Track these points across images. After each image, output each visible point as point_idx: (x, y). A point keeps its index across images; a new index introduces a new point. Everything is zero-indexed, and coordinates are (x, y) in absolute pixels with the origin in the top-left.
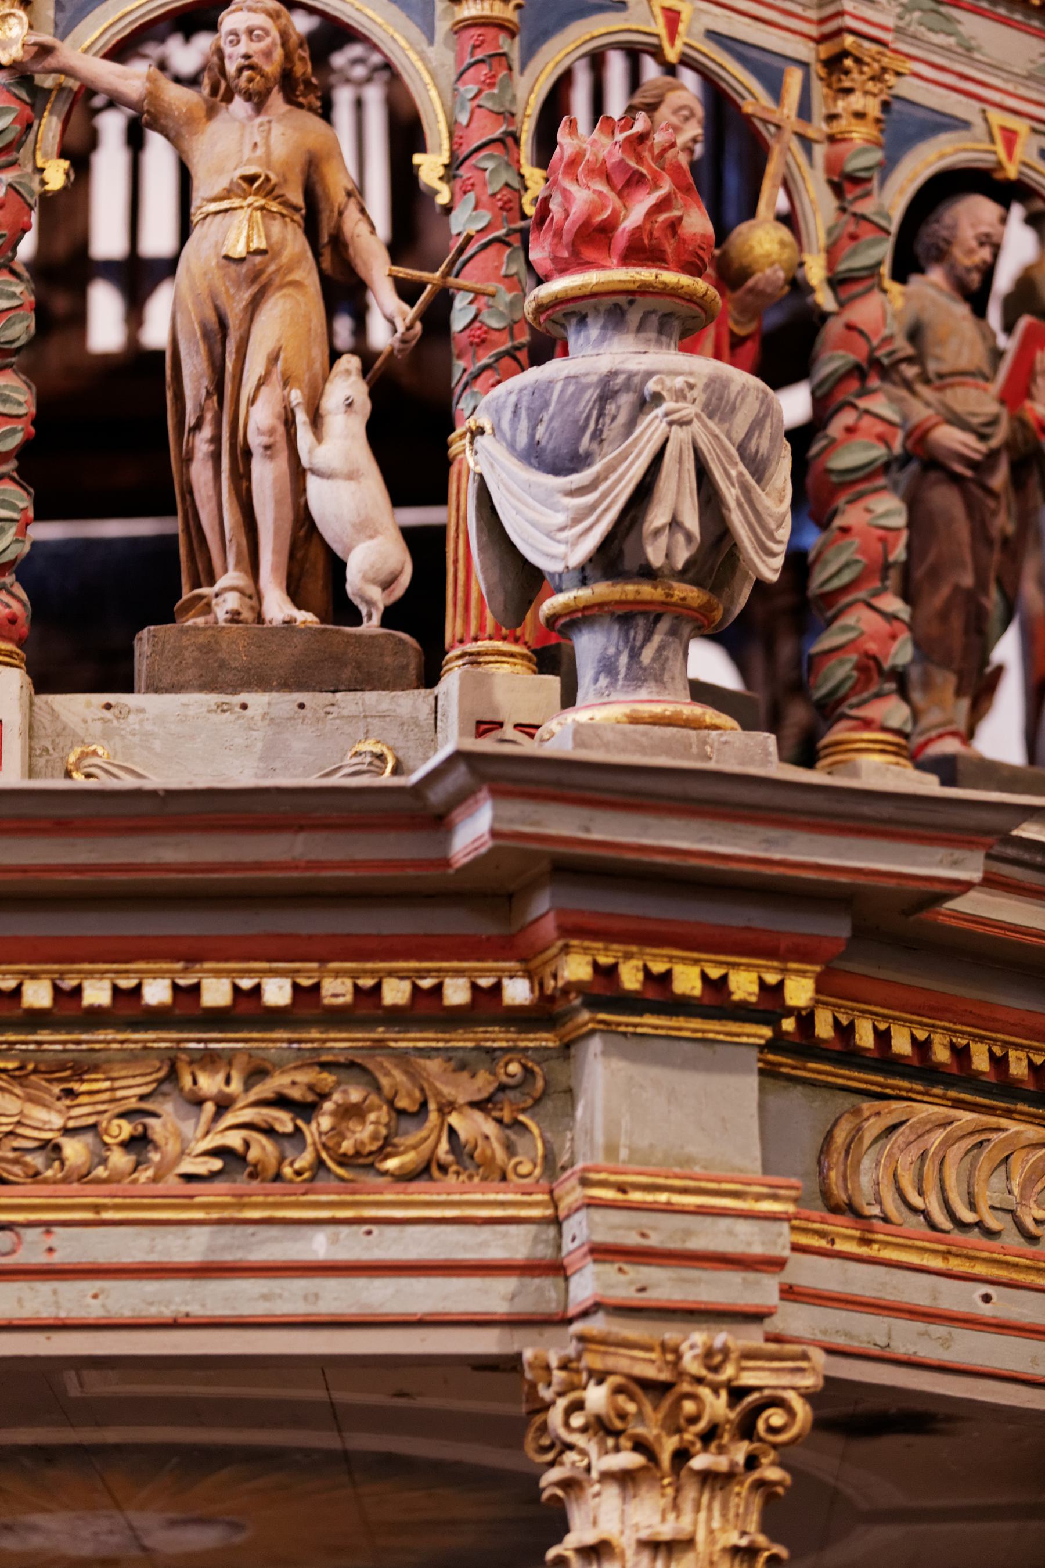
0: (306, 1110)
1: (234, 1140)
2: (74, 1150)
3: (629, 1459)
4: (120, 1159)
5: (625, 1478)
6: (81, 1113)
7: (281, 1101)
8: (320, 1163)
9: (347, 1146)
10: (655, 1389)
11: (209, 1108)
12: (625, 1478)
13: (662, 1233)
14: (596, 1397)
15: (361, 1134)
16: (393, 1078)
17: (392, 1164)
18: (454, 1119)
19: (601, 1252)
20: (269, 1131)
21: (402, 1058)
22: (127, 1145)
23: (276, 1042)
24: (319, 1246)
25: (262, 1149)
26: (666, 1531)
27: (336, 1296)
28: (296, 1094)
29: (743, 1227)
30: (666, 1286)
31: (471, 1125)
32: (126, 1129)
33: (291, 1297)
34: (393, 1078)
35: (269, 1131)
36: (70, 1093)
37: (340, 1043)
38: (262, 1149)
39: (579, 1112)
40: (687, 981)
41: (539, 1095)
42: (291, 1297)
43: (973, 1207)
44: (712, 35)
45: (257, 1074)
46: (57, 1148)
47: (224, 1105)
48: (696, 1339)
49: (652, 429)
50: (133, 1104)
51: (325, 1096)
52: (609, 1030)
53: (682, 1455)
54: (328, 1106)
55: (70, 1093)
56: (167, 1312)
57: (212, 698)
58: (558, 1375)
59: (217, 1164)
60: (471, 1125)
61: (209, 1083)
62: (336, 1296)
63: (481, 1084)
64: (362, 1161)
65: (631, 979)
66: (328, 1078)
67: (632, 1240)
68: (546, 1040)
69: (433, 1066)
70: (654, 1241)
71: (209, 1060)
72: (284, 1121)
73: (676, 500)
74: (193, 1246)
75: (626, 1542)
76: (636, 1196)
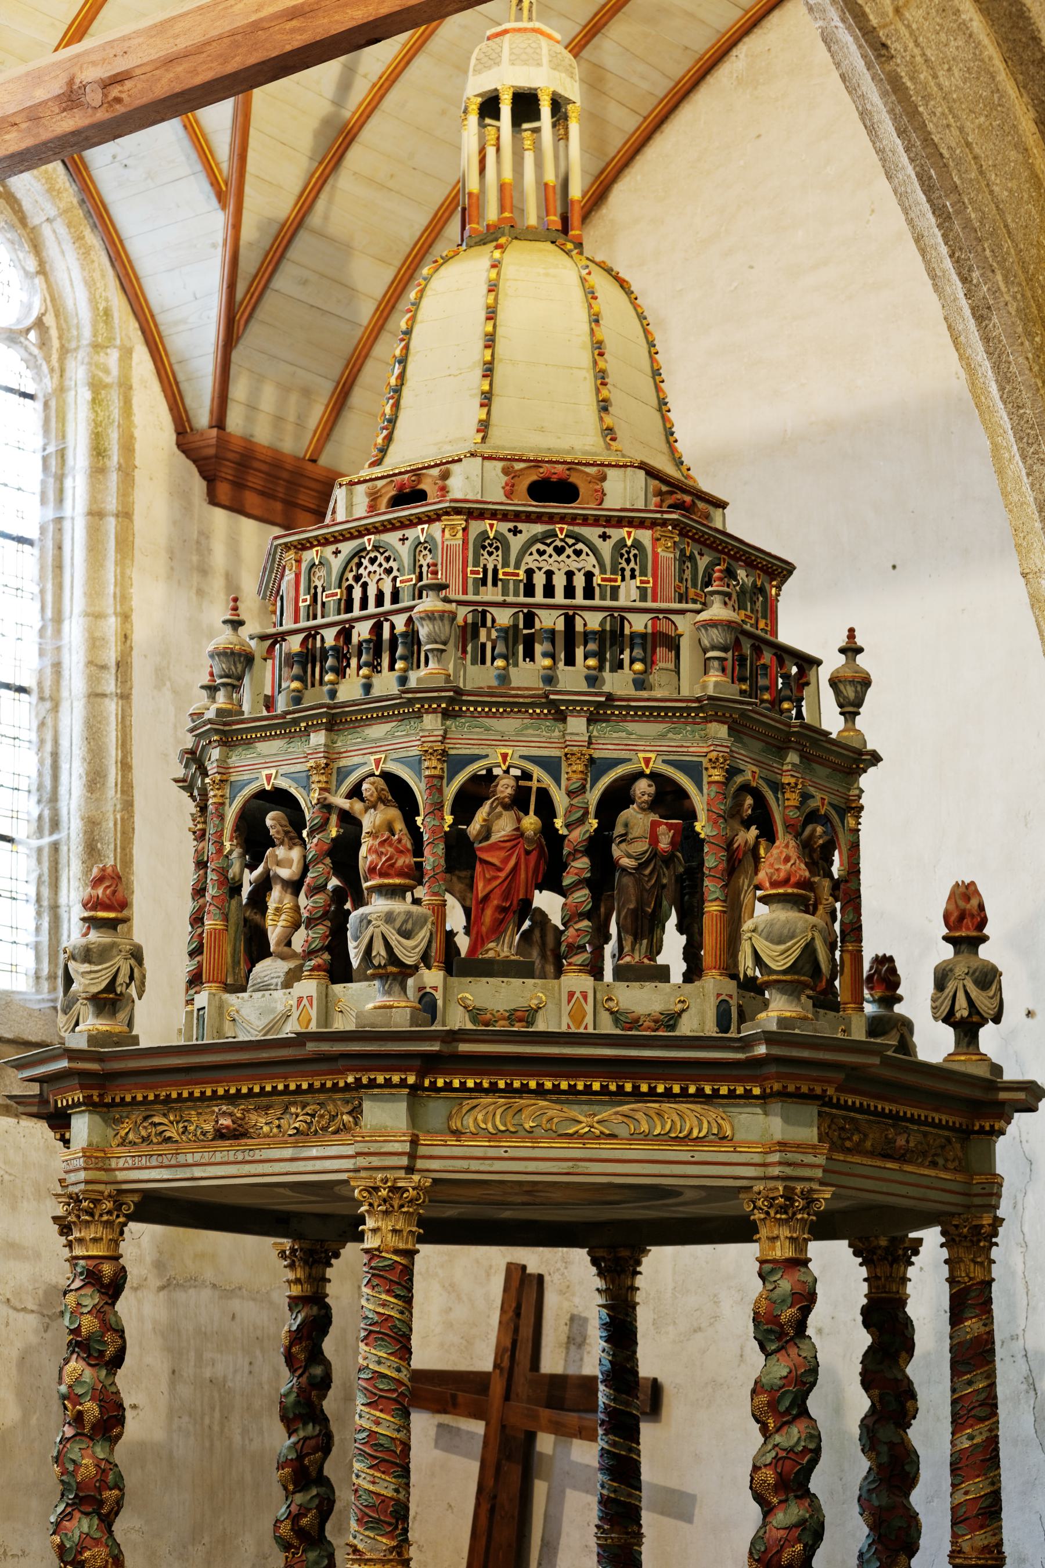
0: (313, 1116)
4: (275, 1130)
13: (374, 1148)
16: (331, 1107)
21: (334, 1101)
23: (308, 1098)
24: (314, 1152)
27: (319, 1165)
29: (396, 1145)
30: (376, 1161)
33: (310, 1166)
40: (380, 1080)
41: (356, 1112)
42: (310, 1166)
44: (521, 757)
47: (297, 1116)
49: (371, 928)
57: (367, 983)
61: (293, 1110)
62: (319, 1165)
63: (350, 1107)
64: (324, 1129)
65: (365, 1081)
71: (294, 1104)
73: (379, 948)
74: (288, 1153)
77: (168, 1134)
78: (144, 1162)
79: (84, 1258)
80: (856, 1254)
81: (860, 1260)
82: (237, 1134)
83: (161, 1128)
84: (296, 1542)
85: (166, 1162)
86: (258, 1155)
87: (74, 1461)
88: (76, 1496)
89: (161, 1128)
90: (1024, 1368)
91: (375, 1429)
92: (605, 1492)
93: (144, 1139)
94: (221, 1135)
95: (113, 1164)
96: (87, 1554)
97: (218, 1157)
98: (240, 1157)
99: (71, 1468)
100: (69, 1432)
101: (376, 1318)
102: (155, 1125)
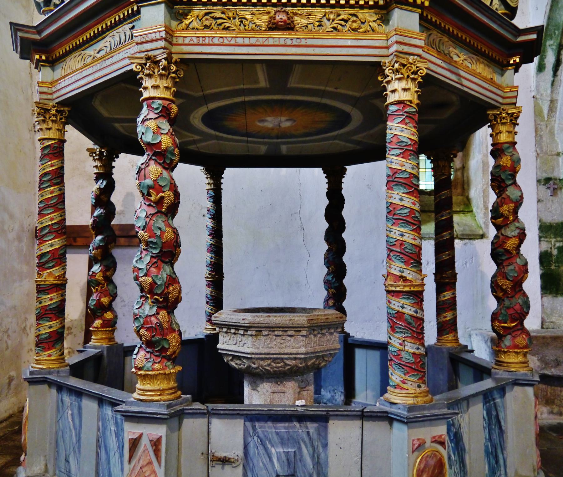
0: (346, 21)
1: (335, 25)
2: (309, 26)
3: (400, 76)
5: (399, 79)
6: (311, 21)
7: (343, 20)
8: (349, 30)
9: (353, 27)
10: (404, 65)
11: (331, 20)
12: (399, 79)
13: (406, 40)
14: (397, 66)
15: (355, 25)
17: (361, 30)
18: (370, 23)
19: (397, 42)
20: (341, 25)
22: (318, 26)
24: (349, 43)
25: (340, 27)
26: (407, 87)
28: (346, 18)
29: (418, 41)
30: (406, 49)
31: (374, 25)
32: (317, 24)
34: (360, 16)
35: (341, 25)
36: (308, 18)
37: (352, 11)
38: (340, 27)
39: (390, 23)
41: (385, 20)
43: (439, 48)
45: (339, 15)
46: (307, 26)
47: (333, 20)
48: (411, 59)
50: (318, 20)
51: (349, 19)
52: (398, 7)
53: (408, 76)
54: (351, 20)
55: (308, 18)
56: (325, 53)
58: (387, 64)
59: (332, 29)
60: (374, 25)
64: (355, 30)
66: (350, 17)
67: (402, 41)
68: (384, 12)
69: (367, 14)
70: (405, 41)
72: (343, 23)
75: (400, 89)
76: (402, 34)
77: (227, 25)
78: (207, 41)
79: (160, 98)
80: (324, 173)
81: (326, 175)
82: (289, 27)
83: (219, 21)
84: (103, 282)
85: (226, 42)
86: (303, 42)
87: (160, 229)
88: (161, 251)
89: (219, 21)
90: (300, 223)
91: (413, 207)
92: (213, 260)
93: (206, 27)
94: (273, 27)
95: (180, 41)
96: (171, 288)
97: (271, 42)
98: (289, 42)
99: (159, 233)
100: (152, 211)
101: (409, 142)
102: (216, 19)
